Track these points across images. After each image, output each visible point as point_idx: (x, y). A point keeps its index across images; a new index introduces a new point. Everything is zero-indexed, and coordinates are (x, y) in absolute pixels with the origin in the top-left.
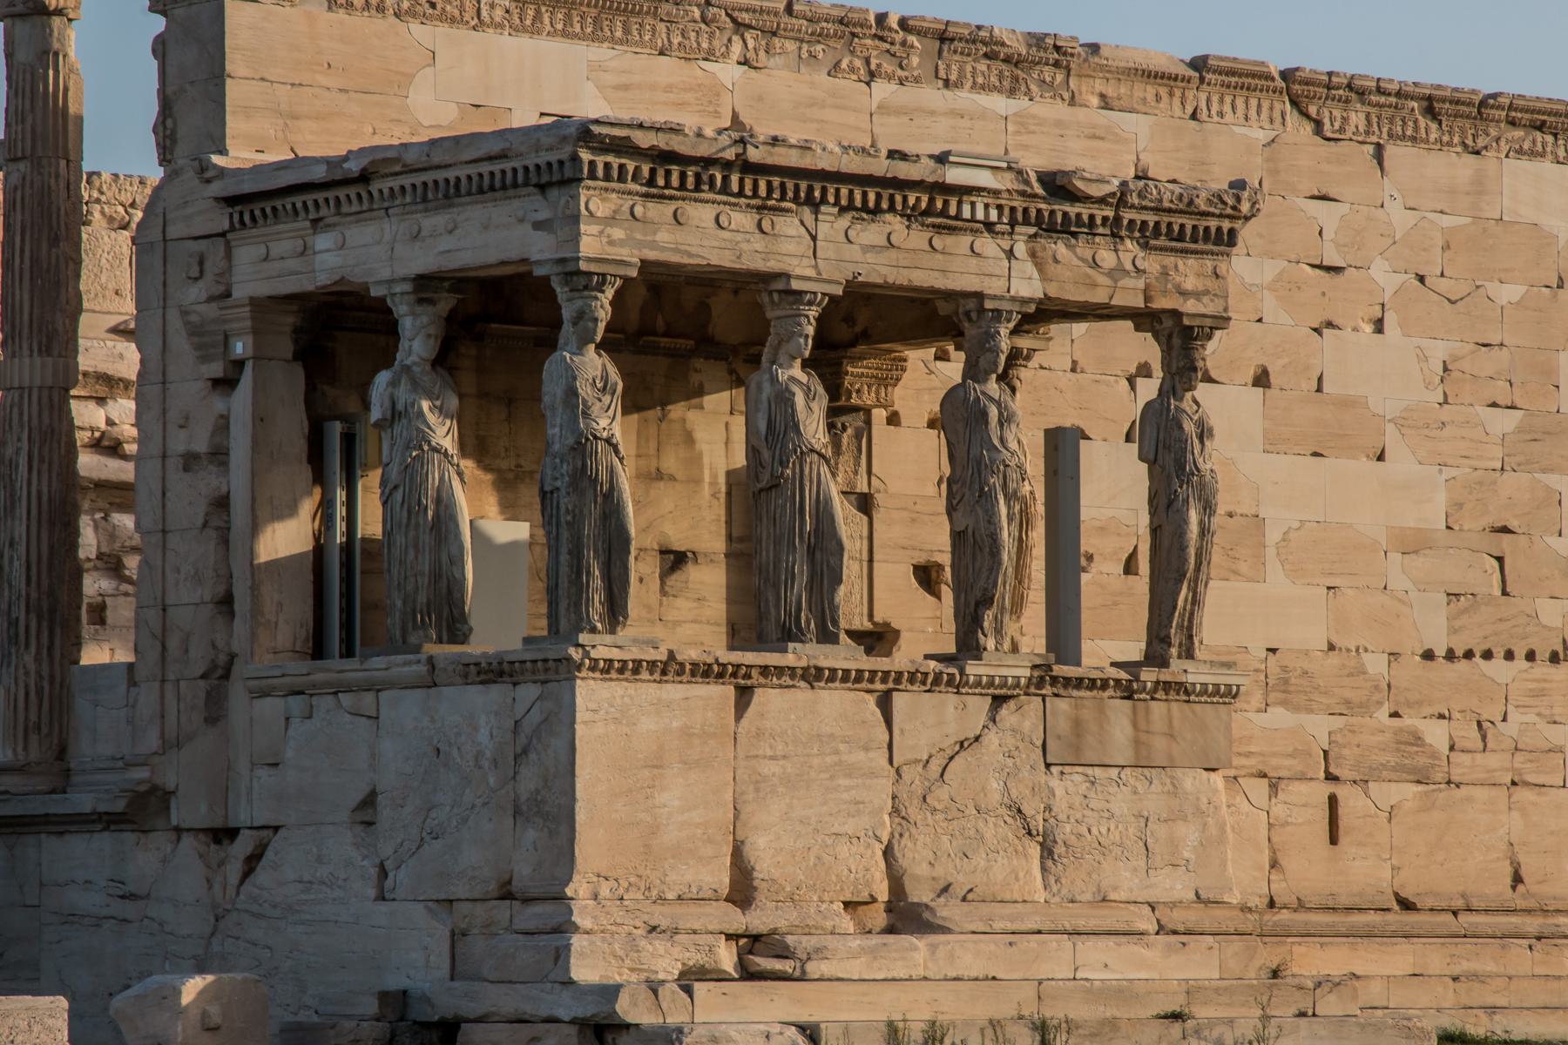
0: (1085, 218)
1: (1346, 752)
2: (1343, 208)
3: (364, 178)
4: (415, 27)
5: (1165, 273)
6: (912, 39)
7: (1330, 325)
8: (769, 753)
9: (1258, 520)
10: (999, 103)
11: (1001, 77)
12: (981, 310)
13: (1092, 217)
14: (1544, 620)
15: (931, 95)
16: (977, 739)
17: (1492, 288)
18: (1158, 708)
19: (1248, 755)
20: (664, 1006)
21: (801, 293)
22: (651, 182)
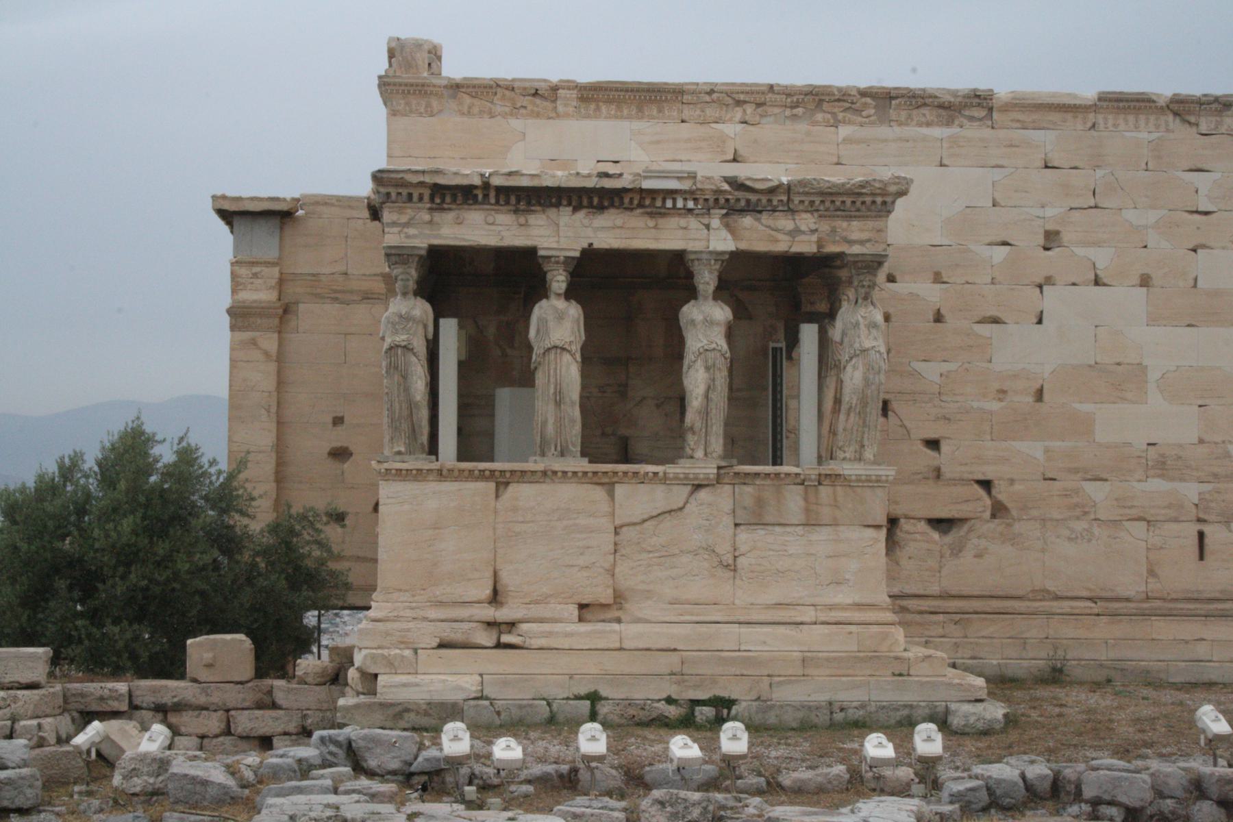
0: (764, 201)
1: (1213, 505)
2: (1217, 176)
5: (834, 230)
6: (869, 100)
7: (1204, 246)
8: (521, 519)
9: (1142, 369)
10: (937, 132)
11: (939, 116)
12: (693, 261)
13: (770, 201)
15: (883, 131)
16: (681, 509)
18: (825, 491)
19: (1133, 507)
20: (396, 664)
21: (549, 257)
22: (432, 200)
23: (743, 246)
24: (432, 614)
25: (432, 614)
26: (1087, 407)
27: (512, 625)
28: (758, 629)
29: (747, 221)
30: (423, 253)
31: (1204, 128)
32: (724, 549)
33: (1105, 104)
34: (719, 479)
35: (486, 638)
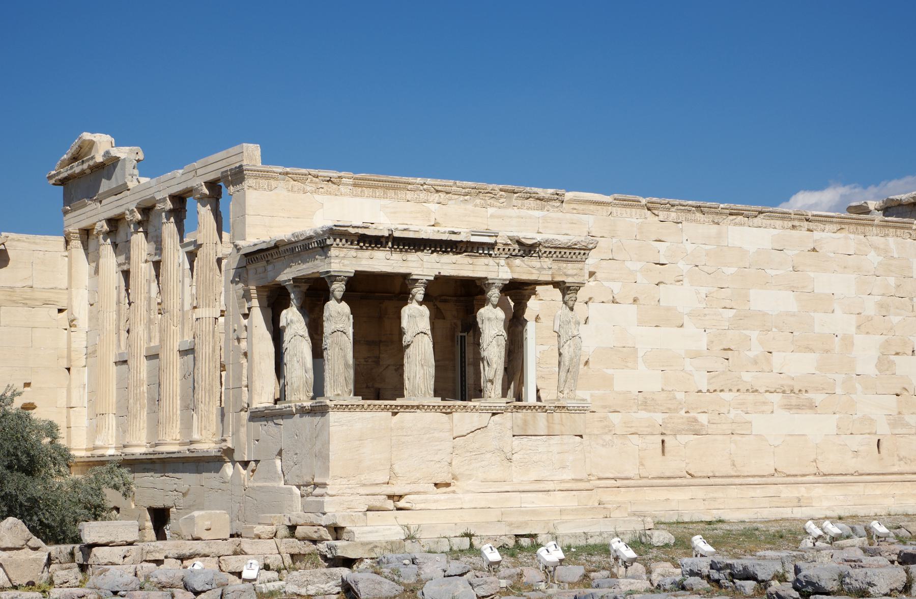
3: (276, 246)
4: (316, 196)
6: (503, 193)
9: (635, 349)
14: (744, 379)
17: (725, 269)
18: (557, 415)
23: (516, 276)
24: (363, 491)
25: (363, 491)
26: (610, 371)
27: (401, 497)
28: (529, 494)
29: (518, 261)
30: (352, 275)
31: (661, 218)
32: (507, 449)
33: (617, 202)
34: (506, 410)
35: (390, 504)
